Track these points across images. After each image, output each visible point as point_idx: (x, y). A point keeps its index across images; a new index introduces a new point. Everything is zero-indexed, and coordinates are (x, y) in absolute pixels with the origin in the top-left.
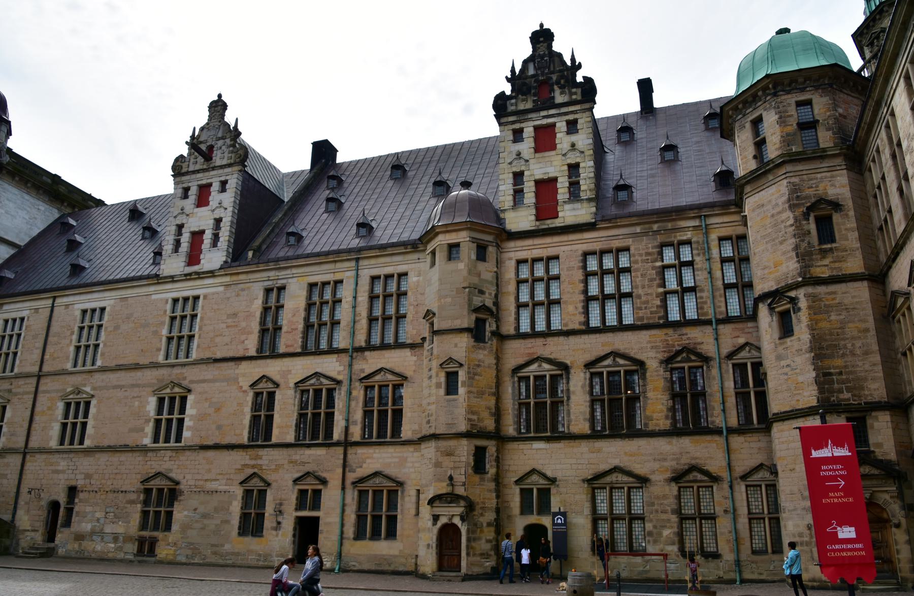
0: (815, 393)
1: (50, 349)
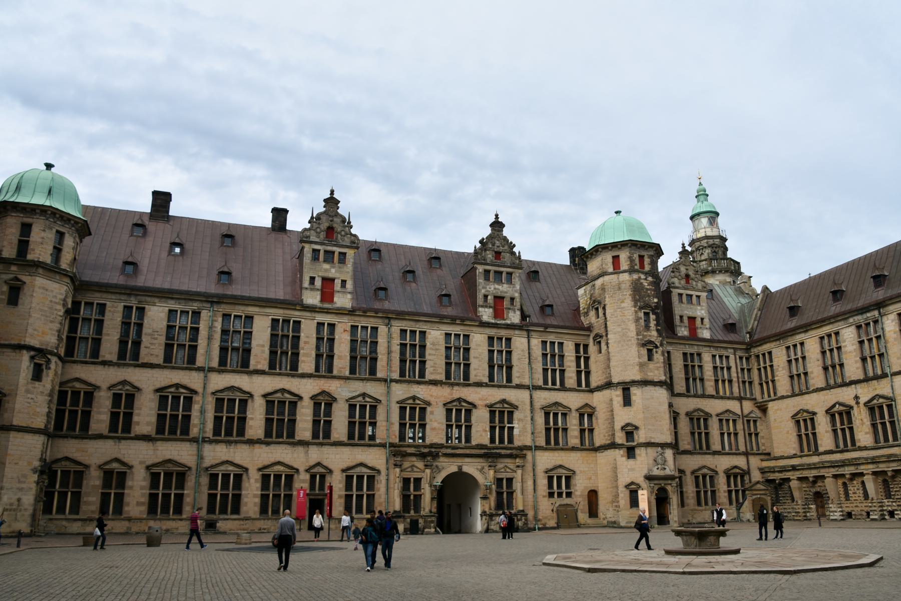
0: (45, 421)
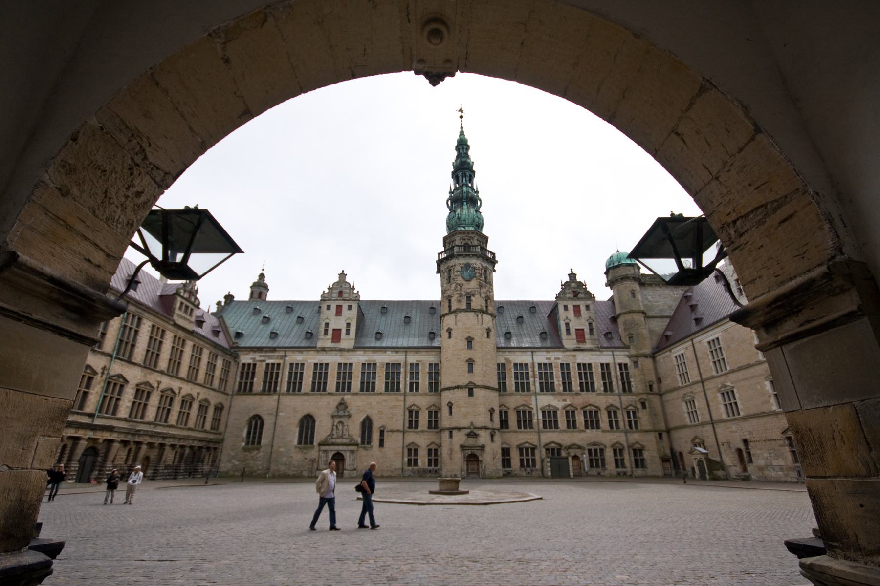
1: (701, 367)
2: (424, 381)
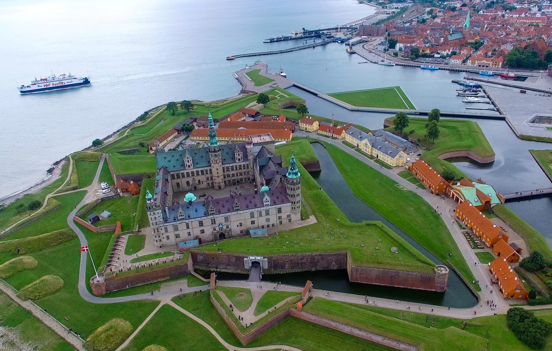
2: (209, 172)
